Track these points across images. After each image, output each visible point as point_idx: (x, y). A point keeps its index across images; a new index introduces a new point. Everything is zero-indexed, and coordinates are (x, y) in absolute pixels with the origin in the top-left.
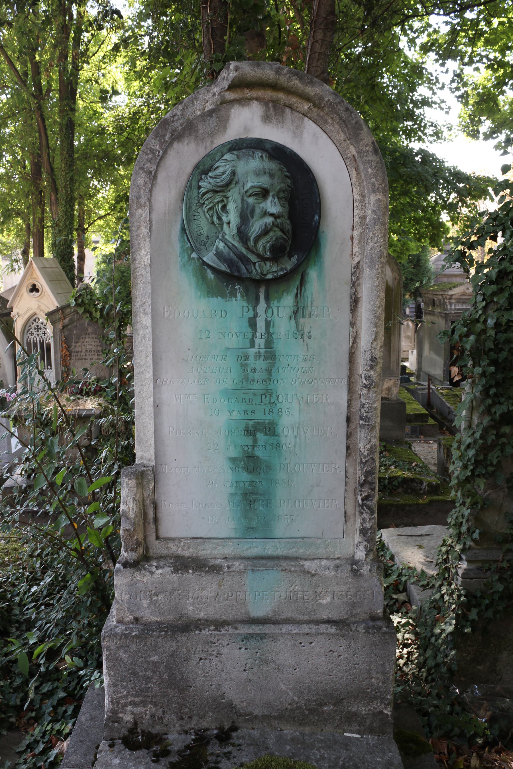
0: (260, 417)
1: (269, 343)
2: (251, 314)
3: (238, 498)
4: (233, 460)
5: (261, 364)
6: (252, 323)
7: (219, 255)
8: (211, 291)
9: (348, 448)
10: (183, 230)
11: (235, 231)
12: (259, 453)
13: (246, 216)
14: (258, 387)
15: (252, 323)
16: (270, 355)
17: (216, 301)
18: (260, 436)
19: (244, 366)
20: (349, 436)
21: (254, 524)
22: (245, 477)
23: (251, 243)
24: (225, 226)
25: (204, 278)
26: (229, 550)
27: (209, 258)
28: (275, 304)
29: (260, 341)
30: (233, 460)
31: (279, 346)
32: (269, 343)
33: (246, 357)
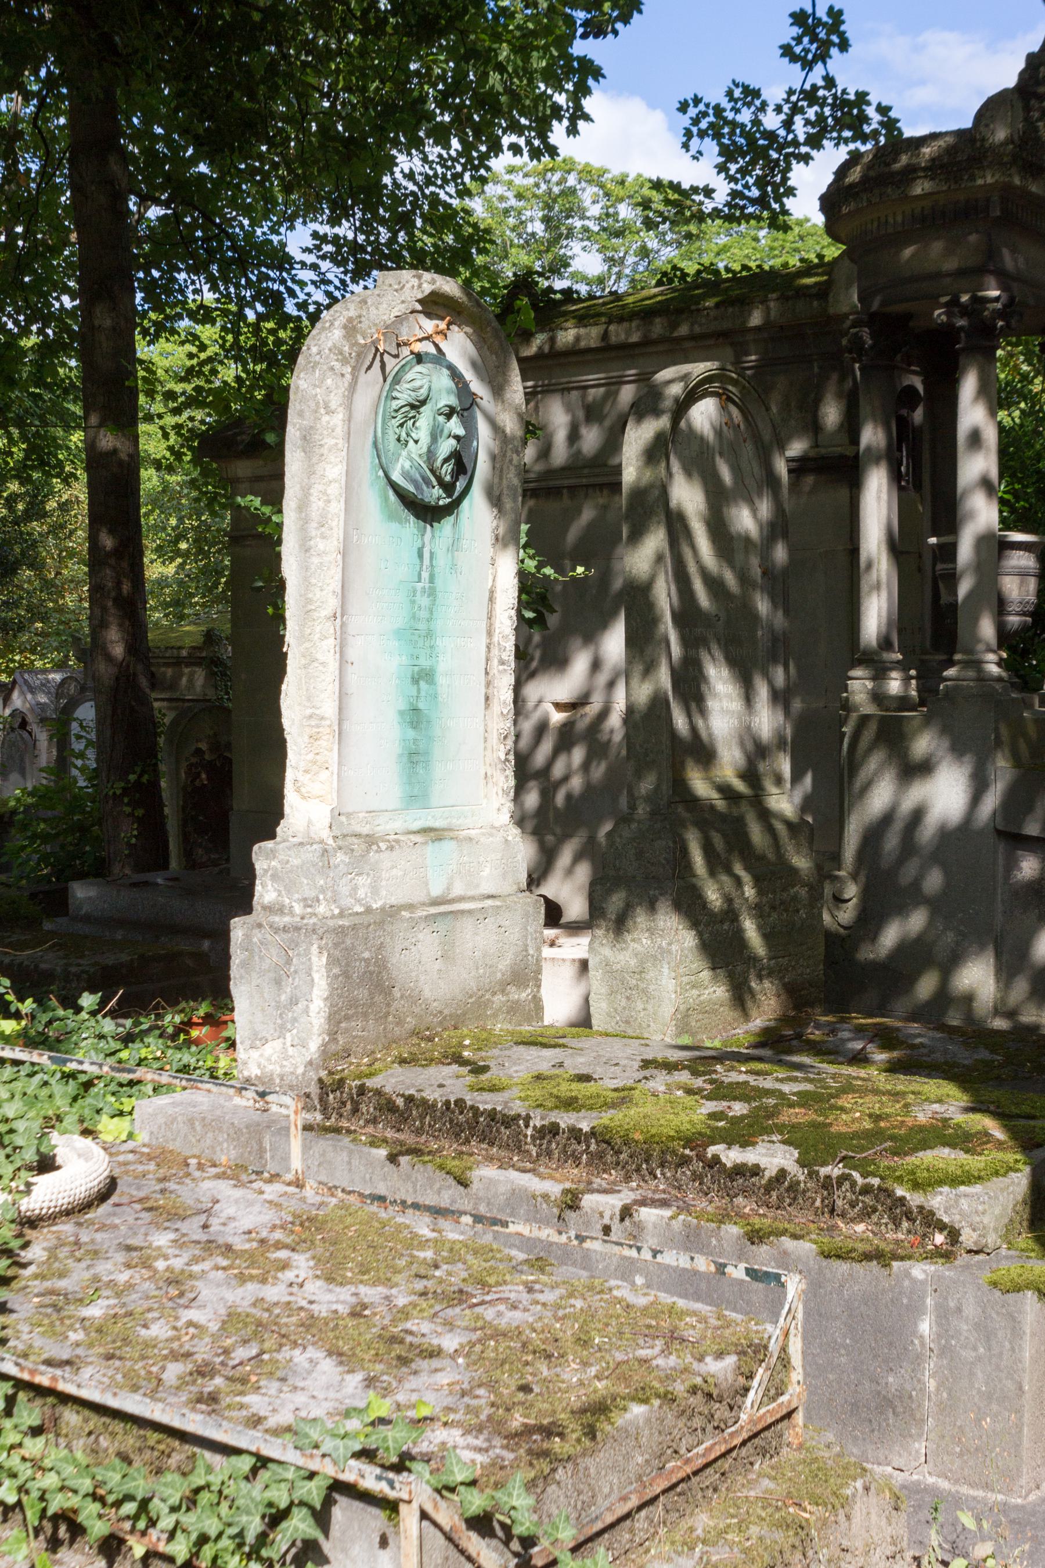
0: (424, 662)
1: (432, 579)
2: (419, 544)
3: (405, 759)
4: (401, 713)
5: (424, 601)
6: (420, 555)
7: (406, 475)
8: (392, 517)
9: (487, 699)
10: (375, 444)
11: (425, 450)
12: (421, 705)
13: (435, 435)
14: (422, 626)
15: (420, 555)
16: (432, 593)
17: (395, 525)
18: (422, 683)
19: (413, 602)
20: (488, 684)
21: (416, 792)
22: (411, 733)
23: (438, 463)
24: (411, 443)
25: (386, 499)
26: (398, 825)
27: (396, 476)
28: (437, 534)
29: (425, 575)
30: (401, 713)
31: (439, 582)
32: (432, 579)
33: (415, 591)
